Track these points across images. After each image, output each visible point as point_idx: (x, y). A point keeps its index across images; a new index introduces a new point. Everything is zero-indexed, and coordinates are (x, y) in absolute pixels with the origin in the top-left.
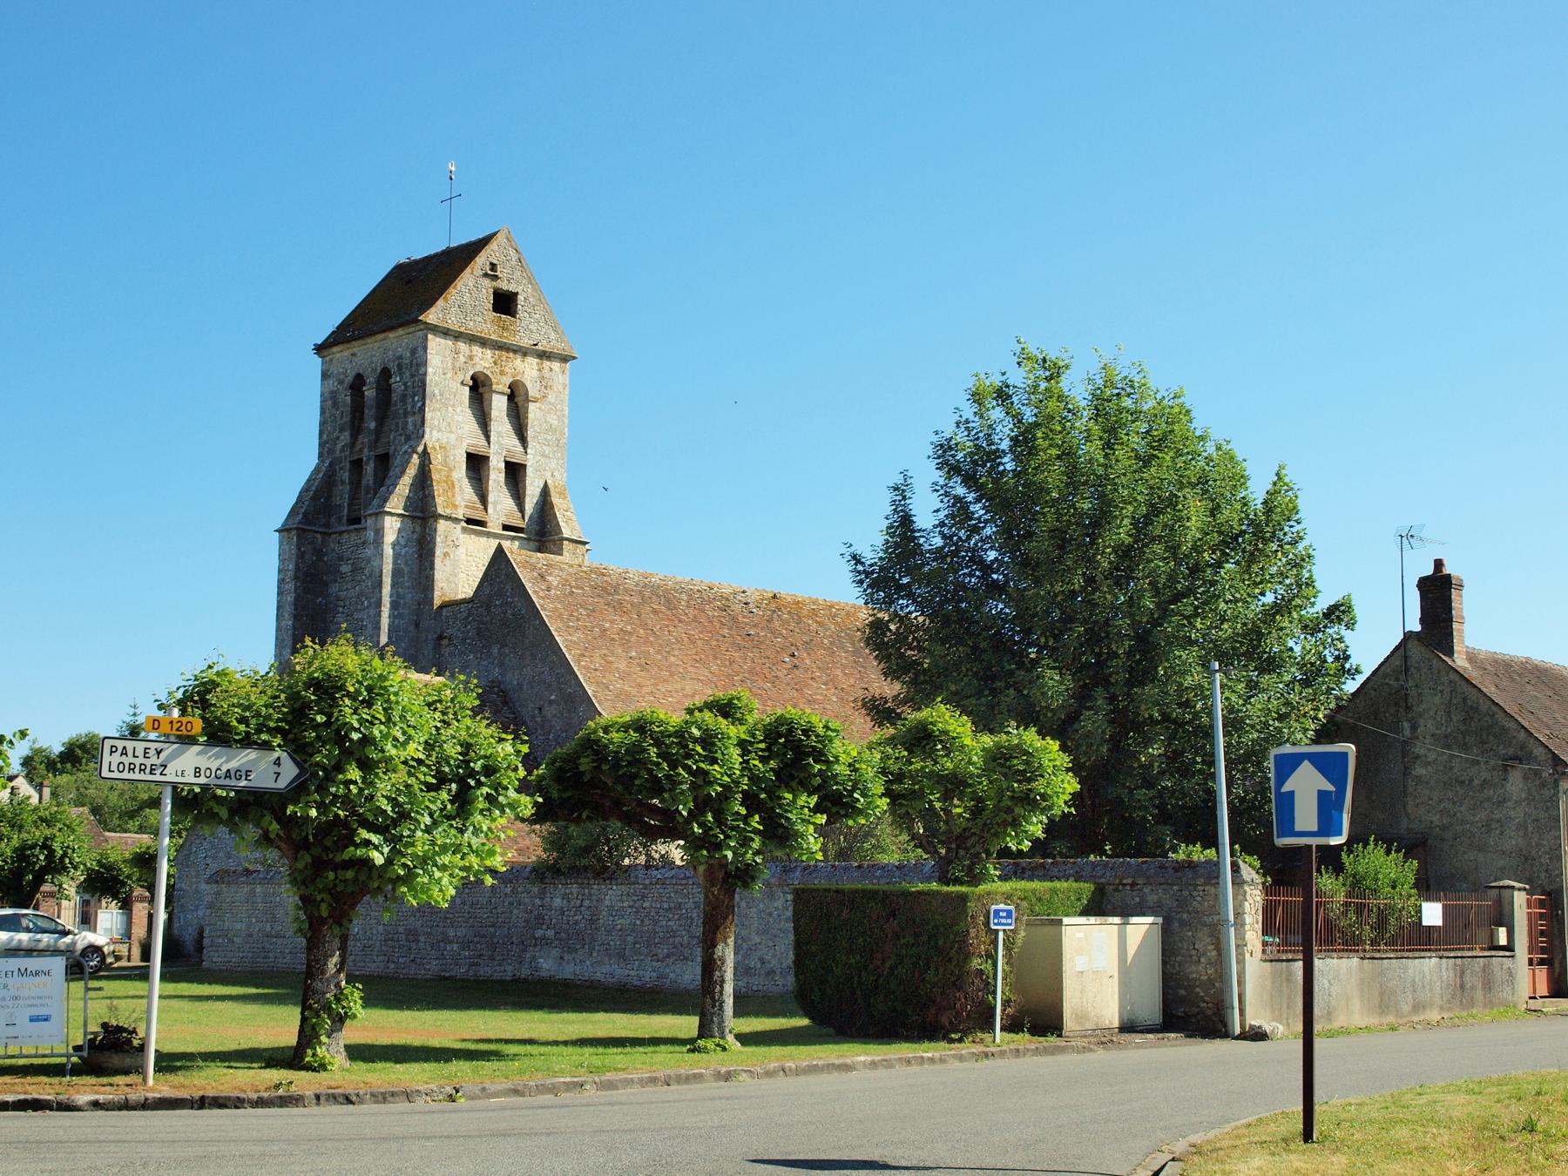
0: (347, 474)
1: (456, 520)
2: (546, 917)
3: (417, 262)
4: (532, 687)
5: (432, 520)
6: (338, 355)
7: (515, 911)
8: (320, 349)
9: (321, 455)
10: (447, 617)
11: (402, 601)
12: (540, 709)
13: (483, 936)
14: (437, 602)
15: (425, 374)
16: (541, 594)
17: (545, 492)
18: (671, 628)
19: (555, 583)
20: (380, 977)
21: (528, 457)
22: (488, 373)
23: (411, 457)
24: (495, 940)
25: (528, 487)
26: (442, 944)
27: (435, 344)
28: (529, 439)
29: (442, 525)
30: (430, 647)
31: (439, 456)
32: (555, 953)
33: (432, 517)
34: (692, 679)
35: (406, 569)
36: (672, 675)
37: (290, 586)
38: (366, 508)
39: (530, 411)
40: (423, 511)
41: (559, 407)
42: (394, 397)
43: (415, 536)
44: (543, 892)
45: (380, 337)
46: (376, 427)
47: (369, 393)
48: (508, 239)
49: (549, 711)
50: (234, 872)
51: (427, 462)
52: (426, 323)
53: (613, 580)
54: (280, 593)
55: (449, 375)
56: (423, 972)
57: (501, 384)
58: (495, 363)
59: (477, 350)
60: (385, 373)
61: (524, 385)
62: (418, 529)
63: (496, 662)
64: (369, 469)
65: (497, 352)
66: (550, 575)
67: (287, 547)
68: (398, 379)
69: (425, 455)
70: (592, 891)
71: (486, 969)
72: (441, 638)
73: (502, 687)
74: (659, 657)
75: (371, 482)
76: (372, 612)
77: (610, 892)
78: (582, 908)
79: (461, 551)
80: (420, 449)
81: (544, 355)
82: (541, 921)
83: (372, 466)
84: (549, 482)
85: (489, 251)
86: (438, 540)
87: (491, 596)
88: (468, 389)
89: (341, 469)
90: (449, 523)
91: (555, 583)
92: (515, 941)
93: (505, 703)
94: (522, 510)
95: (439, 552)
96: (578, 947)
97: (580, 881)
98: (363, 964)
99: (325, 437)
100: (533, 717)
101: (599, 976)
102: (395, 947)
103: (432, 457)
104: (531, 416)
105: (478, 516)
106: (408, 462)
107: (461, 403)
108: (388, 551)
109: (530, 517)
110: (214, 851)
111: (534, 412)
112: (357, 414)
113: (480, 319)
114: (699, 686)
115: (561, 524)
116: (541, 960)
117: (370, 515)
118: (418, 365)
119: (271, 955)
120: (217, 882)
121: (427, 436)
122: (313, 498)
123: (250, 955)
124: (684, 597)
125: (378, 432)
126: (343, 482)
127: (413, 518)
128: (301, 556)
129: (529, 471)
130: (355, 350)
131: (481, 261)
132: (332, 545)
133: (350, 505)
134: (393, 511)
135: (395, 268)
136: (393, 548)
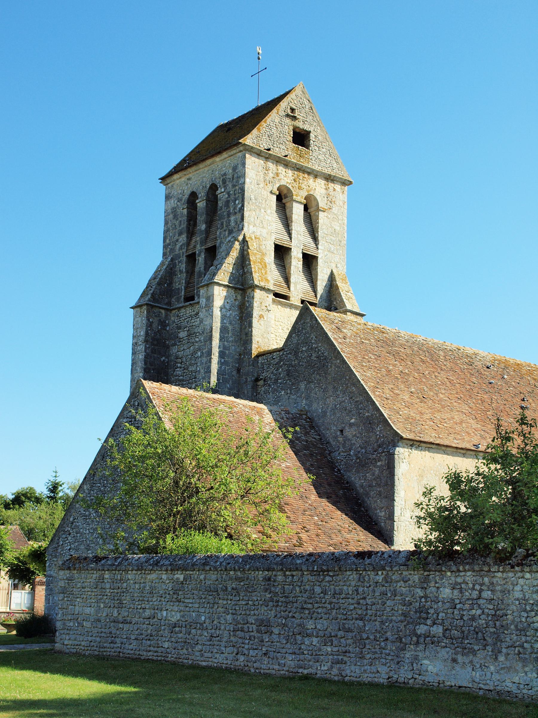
0: (184, 265)
1: (268, 290)
2: (431, 611)
3: (233, 121)
4: (334, 414)
5: (250, 290)
6: (178, 181)
7: (389, 603)
8: (163, 179)
9: (164, 254)
10: (262, 364)
11: (227, 352)
12: (342, 431)
13: (349, 630)
14: (254, 353)
15: (244, 183)
16: (340, 340)
17: (332, 278)
18: (436, 374)
19: (349, 335)
20: (228, 670)
21: (319, 251)
22: (290, 187)
23: (234, 244)
24: (365, 636)
25: (319, 274)
26: (299, 637)
27: (251, 161)
28: (319, 238)
29: (258, 294)
30: (249, 387)
31: (255, 244)
32: (444, 653)
33: (251, 287)
34: (458, 411)
35: (230, 328)
36: (443, 407)
37: (141, 348)
38: (198, 284)
39: (320, 218)
40: (242, 285)
41: (340, 217)
42: (220, 204)
43: (237, 303)
44: (426, 580)
45: (209, 162)
46: (206, 229)
47: (201, 204)
48: (303, 92)
49: (349, 432)
50: (85, 559)
51: (246, 248)
52: (245, 144)
53: (391, 336)
54: (134, 353)
55: (262, 185)
56: (276, 667)
57: (300, 195)
58: (295, 180)
59: (281, 169)
60: (214, 188)
61: (315, 199)
62: (239, 297)
63: (303, 395)
64: (201, 259)
65: (296, 173)
66: (345, 328)
67: (139, 319)
68: (223, 190)
69: (244, 242)
70: (495, 580)
71: (353, 668)
72: (257, 380)
73: (309, 414)
74: (432, 393)
75: (202, 269)
76: (204, 360)
77: (521, 581)
78: (481, 601)
79: (271, 315)
80: (241, 238)
81: (329, 178)
82: (424, 615)
83: (203, 256)
84: (334, 271)
85: (289, 99)
86: (255, 305)
87: (298, 344)
88: (275, 197)
89: (179, 262)
90: (263, 293)
91: (349, 335)
92: (391, 638)
93: (312, 427)
94: (315, 291)
95: (256, 313)
96: (476, 648)
97: (476, 568)
98: (210, 655)
99: (168, 241)
100: (336, 437)
101: (509, 685)
102: (245, 638)
103: (249, 244)
104: (321, 221)
105: (282, 291)
106: (231, 247)
107: (270, 207)
108: (217, 313)
109: (321, 296)
110: (77, 544)
111: (323, 220)
112: (192, 222)
113: (283, 147)
114: (464, 417)
115: (345, 300)
116: (426, 662)
117: (202, 287)
118: (239, 177)
119: (118, 640)
120: (69, 568)
121: (245, 229)
122: (159, 284)
123: (98, 639)
124: (441, 353)
125: (208, 232)
126: (181, 272)
127: (235, 289)
128: (150, 325)
129: (320, 261)
130: (191, 175)
131: (283, 104)
132: (172, 318)
133: (186, 288)
134: (221, 282)
135: (218, 127)
136: (221, 311)
